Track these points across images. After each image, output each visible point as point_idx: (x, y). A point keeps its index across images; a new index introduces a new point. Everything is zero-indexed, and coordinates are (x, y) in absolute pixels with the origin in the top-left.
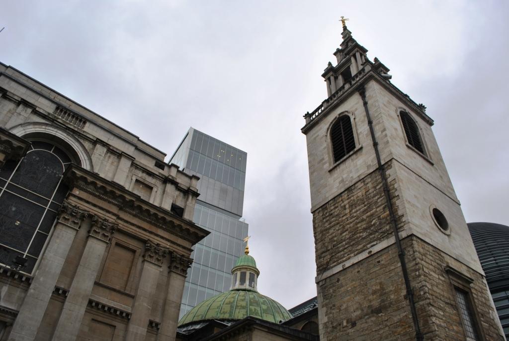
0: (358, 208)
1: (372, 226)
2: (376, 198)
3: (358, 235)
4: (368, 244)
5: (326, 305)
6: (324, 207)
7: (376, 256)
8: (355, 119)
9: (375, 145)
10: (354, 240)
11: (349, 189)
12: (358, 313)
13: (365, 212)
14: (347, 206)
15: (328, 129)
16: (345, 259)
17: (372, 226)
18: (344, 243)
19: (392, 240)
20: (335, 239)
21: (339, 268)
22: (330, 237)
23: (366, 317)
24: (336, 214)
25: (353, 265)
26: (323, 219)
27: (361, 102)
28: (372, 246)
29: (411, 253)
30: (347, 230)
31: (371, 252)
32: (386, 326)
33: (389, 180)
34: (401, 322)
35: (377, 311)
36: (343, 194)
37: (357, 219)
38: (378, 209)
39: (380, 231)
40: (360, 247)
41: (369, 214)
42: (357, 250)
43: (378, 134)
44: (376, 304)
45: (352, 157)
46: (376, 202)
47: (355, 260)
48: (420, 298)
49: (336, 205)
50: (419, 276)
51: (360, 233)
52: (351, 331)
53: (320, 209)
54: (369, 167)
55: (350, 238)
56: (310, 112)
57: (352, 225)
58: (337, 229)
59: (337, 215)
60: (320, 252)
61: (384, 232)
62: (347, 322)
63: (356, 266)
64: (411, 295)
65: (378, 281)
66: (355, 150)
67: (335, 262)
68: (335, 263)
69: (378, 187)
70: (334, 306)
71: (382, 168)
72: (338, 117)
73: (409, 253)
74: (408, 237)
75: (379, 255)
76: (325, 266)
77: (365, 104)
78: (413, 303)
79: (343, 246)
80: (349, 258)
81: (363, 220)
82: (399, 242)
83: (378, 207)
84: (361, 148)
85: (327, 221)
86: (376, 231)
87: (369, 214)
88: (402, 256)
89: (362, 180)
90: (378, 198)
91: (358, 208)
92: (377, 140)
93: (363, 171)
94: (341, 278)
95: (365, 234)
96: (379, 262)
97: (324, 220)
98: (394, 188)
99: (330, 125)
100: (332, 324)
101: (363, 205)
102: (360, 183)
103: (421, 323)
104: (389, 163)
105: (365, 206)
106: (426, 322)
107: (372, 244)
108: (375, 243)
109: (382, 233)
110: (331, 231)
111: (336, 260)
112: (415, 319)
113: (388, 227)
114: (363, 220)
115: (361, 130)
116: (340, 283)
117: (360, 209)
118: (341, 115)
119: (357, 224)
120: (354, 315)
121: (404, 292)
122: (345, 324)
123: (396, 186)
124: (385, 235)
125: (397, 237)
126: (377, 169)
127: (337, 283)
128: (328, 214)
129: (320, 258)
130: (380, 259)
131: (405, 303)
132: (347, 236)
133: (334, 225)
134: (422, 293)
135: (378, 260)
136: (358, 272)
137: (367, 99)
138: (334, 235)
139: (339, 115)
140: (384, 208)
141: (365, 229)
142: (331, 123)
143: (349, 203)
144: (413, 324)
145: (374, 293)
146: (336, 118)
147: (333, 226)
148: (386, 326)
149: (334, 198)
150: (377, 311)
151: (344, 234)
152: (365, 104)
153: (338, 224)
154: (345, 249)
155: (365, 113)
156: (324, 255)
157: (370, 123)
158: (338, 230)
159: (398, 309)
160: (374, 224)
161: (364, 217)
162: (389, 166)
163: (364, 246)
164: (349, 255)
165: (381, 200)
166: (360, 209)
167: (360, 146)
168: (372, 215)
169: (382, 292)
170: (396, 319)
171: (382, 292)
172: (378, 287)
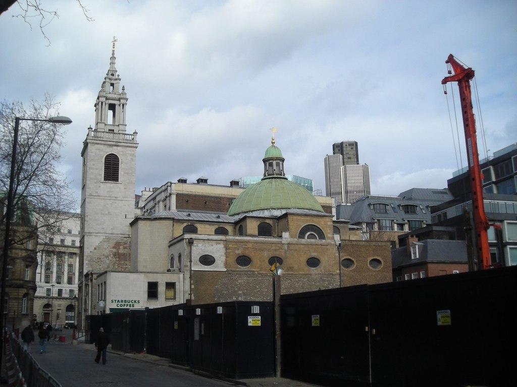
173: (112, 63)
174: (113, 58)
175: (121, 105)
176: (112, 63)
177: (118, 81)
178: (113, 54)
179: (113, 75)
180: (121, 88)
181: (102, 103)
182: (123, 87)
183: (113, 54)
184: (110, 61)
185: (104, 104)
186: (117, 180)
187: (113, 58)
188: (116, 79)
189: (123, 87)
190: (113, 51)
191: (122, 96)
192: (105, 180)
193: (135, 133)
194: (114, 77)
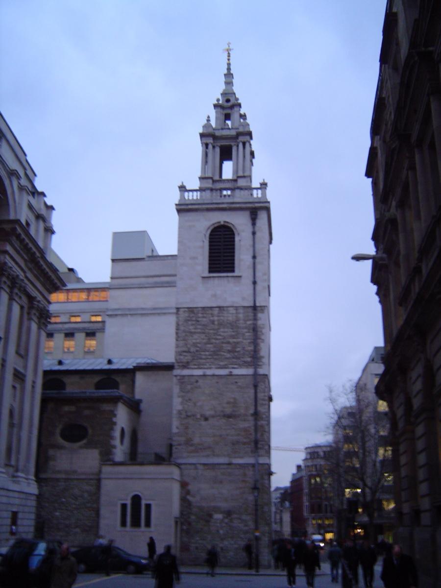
0: (226, 330)
1: (236, 352)
2: (245, 330)
3: (222, 353)
4: (230, 365)
5: (182, 397)
6: (191, 310)
7: (234, 377)
8: (240, 240)
9: (255, 283)
10: (218, 355)
11: (220, 308)
12: (212, 413)
13: (233, 337)
14: (216, 323)
15: (209, 228)
16: (205, 367)
17: (236, 352)
18: (207, 353)
19: (250, 371)
20: (199, 345)
21: (199, 372)
22: (194, 341)
23: (218, 418)
24: (203, 323)
25: (214, 375)
26: (189, 320)
28: (233, 368)
29: (263, 387)
30: (212, 344)
31: (231, 372)
32: (233, 428)
33: (260, 322)
34: (245, 430)
35: (229, 416)
36: (215, 309)
37: (223, 339)
38: (244, 341)
39: (242, 359)
40: (222, 363)
41: (235, 340)
42: (219, 365)
43: (258, 274)
44: (228, 410)
45: (230, 279)
46: (243, 335)
48: (262, 419)
49: (205, 315)
50: (265, 404)
51: (225, 352)
52: (203, 423)
53: (186, 309)
54: (244, 299)
55: (214, 351)
56: (188, 188)
57: (217, 341)
58: (202, 337)
59: (204, 325)
60: (180, 349)
61: (245, 362)
62: (202, 416)
63: (215, 377)
64: (256, 414)
65: (233, 396)
66: (235, 274)
67: (195, 365)
68: (196, 367)
69: (249, 323)
70: (190, 400)
71: (255, 308)
72: (222, 223)
73: (261, 387)
74: (264, 375)
75: (237, 377)
76: (184, 364)
77: (254, 233)
78: (256, 420)
79: (205, 355)
80: (210, 368)
81: (228, 343)
82: (255, 375)
83: (246, 339)
84: (240, 277)
85: (192, 325)
86: (239, 358)
87: (235, 340)
88: (255, 387)
89: (236, 308)
90: (247, 332)
91: (226, 330)
92: (257, 280)
93: (239, 301)
94: (201, 382)
95: (228, 355)
96: (236, 382)
97: (190, 323)
98: (261, 331)
99: (211, 226)
100: (186, 412)
101: (231, 330)
102: (231, 309)
103: (259, 435)
104: (263, 308)
105: (233, 332)
106: (262, 435)
107: (235, 366)
108: (235, 366)
109: (243, 361)
110: (196, 336)
111: (196, 363)
112: (256, 430)
113: (249, 359)
114: (228, 343)
116: (198, 384)
117: (227, 332)
118: (226, 224)
119: (223, 343)
120: (208, 413)
121: (252, 411)
122: (199, 416)
123: (264, 331)
124: (246, 365)
126: (251, 307)
127: (195, 383)
128: (194, 319)
129: (181, 355)
130: (238, 381)
131: (251, 418)
132: (212, 350)
133: (200, 333)
134: (264, 416)
135: (236, 381)
136: (217, 382)
137: (257, 229)
138: (198, 341)
139: (225, 222)
140: (250, 343)
141: (229, 351)
142: (213, 224)
143: (218, 320)
144: (253, 434)
145: (228, 403)
146: (220, 222)
147: (198, 333)
148: (233, 428)
149: (204, 308)
150: (229, 416)
151: (209, 346)
152: (254, 233)
153: (203, 333)
154: (208, 358)
155: (251, 243)
156: (185, 354)
157: (254, 257)
158: (203, 339)
159: (245, 420)
160: (238, 352)
161: (231, 340)
162: (262, 310)
163: (226, 365)
164: (210, 365)
165: (250, 336)
166: (227, 332)
167: (239, 275)
168: (238, 343)
169: (234, 403)
170: (241, 426)
171: (234, 403)
172: (232, 400)
174: (229, 75)
175: (241, 146)
177: (236, 109)
178: (229, 69)
179: (228, 101)
181: (207, 145)
183: (229, 69)
184: (223, 79)
185: (210, 147)
186: (233, 271)
187: (229, 75)
188: (232, 107)
190: (229, 64)
191: (241, 130)
192: (210, 272)
193: (264, 186)
194: (229, 104)
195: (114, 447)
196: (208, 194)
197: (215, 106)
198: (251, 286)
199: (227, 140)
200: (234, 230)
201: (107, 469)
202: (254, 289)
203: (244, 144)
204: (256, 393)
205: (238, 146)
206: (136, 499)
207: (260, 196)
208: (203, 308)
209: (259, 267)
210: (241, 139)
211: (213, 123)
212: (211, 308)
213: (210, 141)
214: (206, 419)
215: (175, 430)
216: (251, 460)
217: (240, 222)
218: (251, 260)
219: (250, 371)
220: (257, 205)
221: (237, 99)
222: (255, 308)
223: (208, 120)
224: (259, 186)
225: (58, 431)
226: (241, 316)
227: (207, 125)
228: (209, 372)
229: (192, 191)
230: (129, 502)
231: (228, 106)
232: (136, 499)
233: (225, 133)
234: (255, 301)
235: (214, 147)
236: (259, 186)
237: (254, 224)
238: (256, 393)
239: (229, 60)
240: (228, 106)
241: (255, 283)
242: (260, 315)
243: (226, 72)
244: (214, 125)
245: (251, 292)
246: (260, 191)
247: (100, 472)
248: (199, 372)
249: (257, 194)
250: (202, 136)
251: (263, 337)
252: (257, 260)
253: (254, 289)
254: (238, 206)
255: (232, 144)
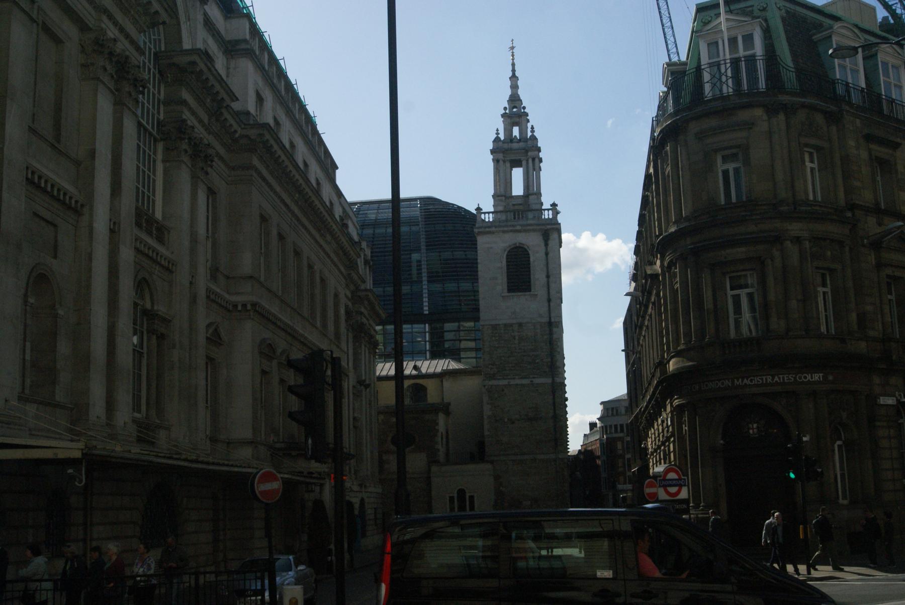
9: (549, 301)
19: (549, 381)
21: (505, 382)
27: (544, 251)
33: (555, 336)
43: (552, 292)
47: (518, 382)
77: (547, 254)
88: (554, 393)
115: (538, 276)
125: (553, 378)
152: (547, 254)
157: (548, 277)
173: (514, 87)
174: (514, 78)
175: (530, 161)
176: (514, 87)
178: (514, 71)
180: (529, 130)
182: (532, 128)
183: (514, 71)
184: (509, 83)
185: (501, 162)
187: (514, 78)
189: (532, 128)
190: (513, 65)
192: (509, 290)
193: (554, 205)
195: (439, 450)
196: (503, 217)
197: (503, 116)
198: (547, 304)
199: (516, 150)
200: (530, 252)
201: (434, 469)
202: (549, 305)
203: (533, 159)
204: (554, 398)
205: (527, 161)
206: (461, 493)
207: (551, 217)
208: (505, 325)
209: (552, 286)
210: (530, 154)
211: (502, 137)
212: (511, 325)
213: (500, 156)
214: (513, 423)
215: (486, 433)
216: (553, 456)
217: (532, 241)
218: (545, 279)
219: (549, 381)
220: (549, 227)
221: (524, 108)
222: (550, 323)
223: (498, 134)
224: (550, 207)
225: (389, 439)
226: (538, 331)
227: (497, 140)
228: (512, 382)
229: (489, 213)
230: (456, 495)
231: (515, 114)
232: (461, 493)
233: (515, 146)
234: (550, 318)
235: (504, 162)
236: (550, 207)
237: (546, 245)
238: (554, 398)
239: (513, 59)
240: (515, 114)
241: (549, 301)
242: (555, 330)
243: (510, 74)
244: (502, 138)
245: (546, 309)
246: (550, 212)
247: (429, 471)
248: (505, 382)
249: (548, 215)
250: (492, 152)
251: (559, 350)
252: (551, 279)
253: (549, 305)
254: (531, 228)
255: (522, 158)
